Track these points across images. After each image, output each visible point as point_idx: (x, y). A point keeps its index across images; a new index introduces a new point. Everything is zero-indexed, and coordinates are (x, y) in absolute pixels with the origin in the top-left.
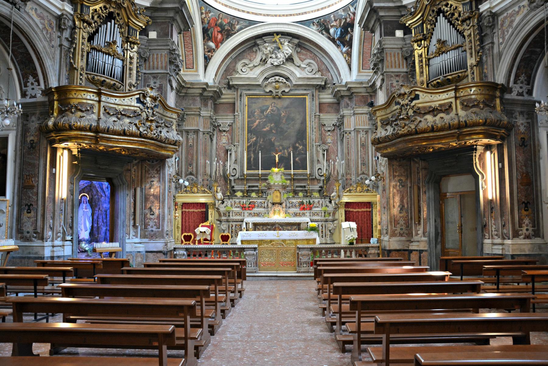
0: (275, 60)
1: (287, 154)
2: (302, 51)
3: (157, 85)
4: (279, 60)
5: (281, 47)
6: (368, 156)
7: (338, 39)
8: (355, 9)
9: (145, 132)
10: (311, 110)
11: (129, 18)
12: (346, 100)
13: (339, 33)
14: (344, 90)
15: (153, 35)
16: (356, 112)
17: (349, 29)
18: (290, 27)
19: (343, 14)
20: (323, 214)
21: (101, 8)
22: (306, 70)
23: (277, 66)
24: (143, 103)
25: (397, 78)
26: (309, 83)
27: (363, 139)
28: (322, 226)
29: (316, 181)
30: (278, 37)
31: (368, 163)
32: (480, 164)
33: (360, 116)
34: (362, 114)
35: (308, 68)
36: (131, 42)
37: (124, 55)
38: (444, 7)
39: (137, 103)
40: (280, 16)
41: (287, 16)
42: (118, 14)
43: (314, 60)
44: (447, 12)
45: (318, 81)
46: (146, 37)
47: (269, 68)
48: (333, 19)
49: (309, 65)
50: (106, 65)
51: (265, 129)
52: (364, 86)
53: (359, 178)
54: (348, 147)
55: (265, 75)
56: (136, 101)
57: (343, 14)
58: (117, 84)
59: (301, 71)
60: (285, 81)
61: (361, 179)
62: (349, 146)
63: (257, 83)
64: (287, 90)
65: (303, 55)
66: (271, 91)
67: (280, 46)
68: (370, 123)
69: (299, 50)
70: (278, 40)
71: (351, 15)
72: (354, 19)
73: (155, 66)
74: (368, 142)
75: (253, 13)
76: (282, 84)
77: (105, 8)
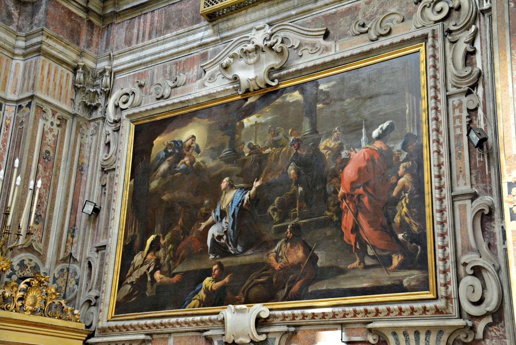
16: (44, 47)
31: (50, 218)
33: (54, 65)
34: (62, 62)
61: (22, 265)
68: (79, 99)
74: (60, 152)
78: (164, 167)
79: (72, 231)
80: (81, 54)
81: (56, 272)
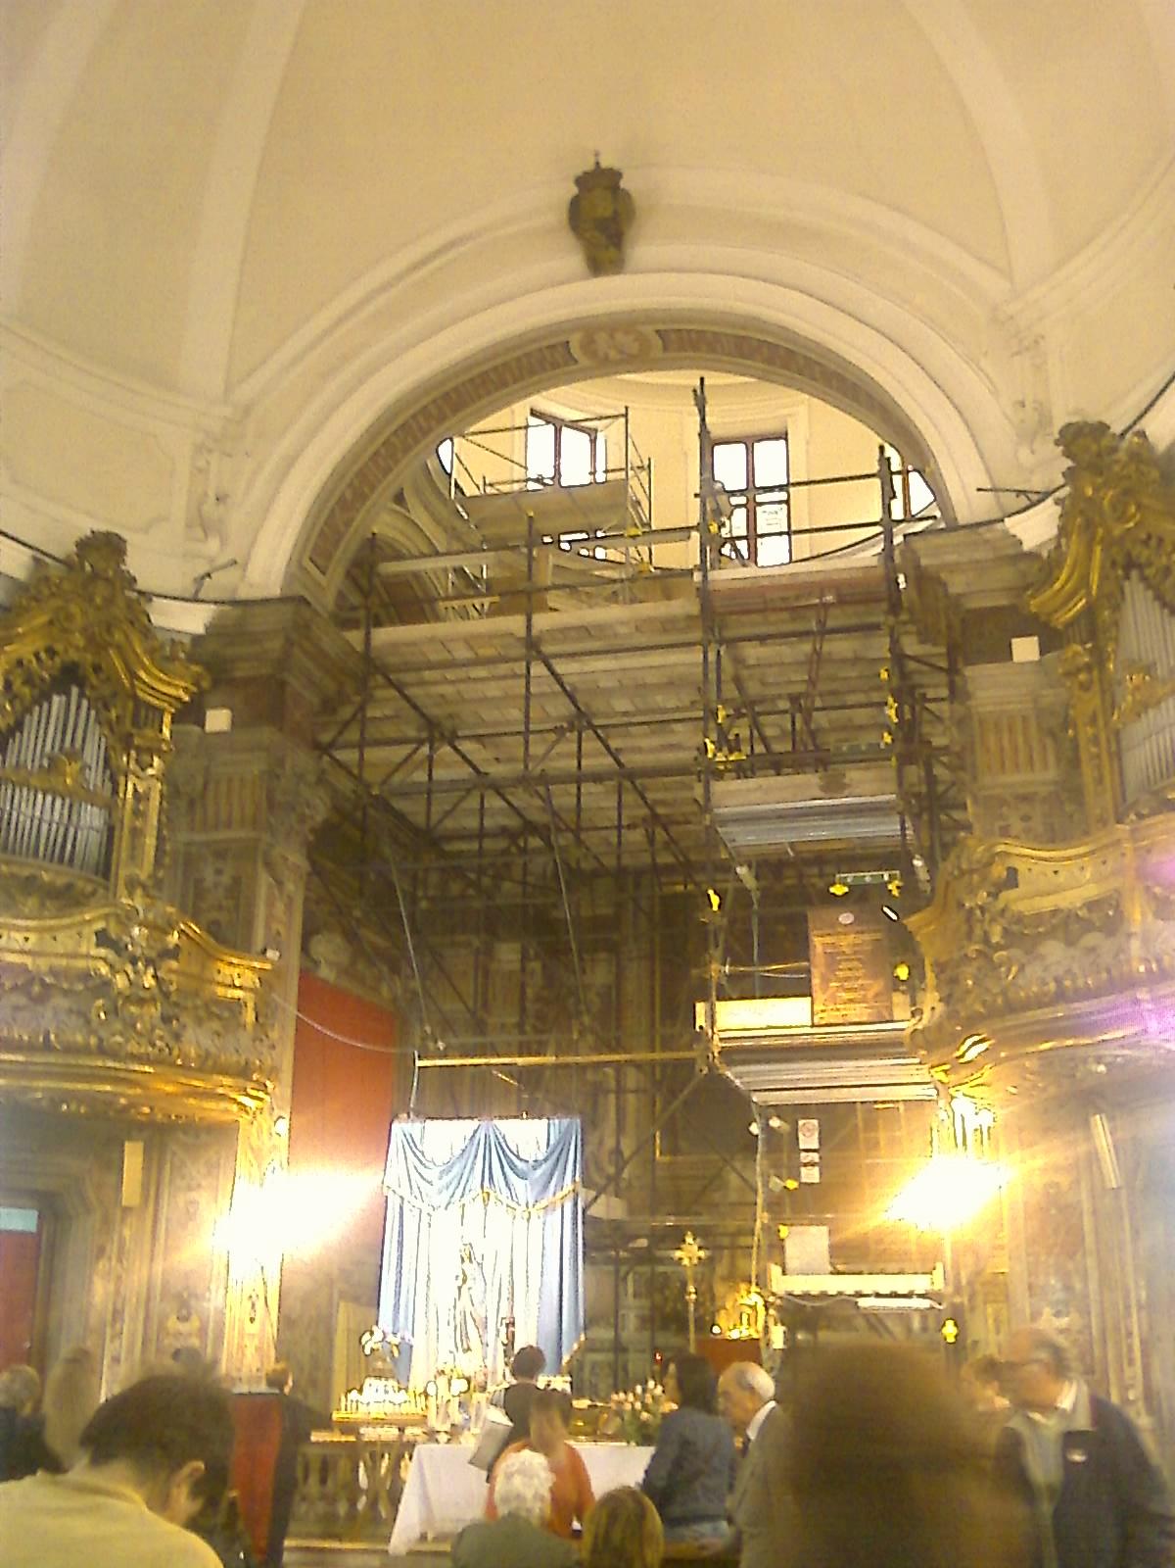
3: (226, 879)
9: (119, 1039)
11: (133, 676)
15: (218, 720)
21: (37, 655)
24: (117, 947)
25: (1025, 808)
36: (139, 750)
37: (115, 792)
39: (98, 945)
42: (97, 669)
44: (1150, 564)
46: (196, 729)
50: (45, 827)
56: (94, 938)
58: (80, 884)
73: (223, 816)
77: (51, 652)
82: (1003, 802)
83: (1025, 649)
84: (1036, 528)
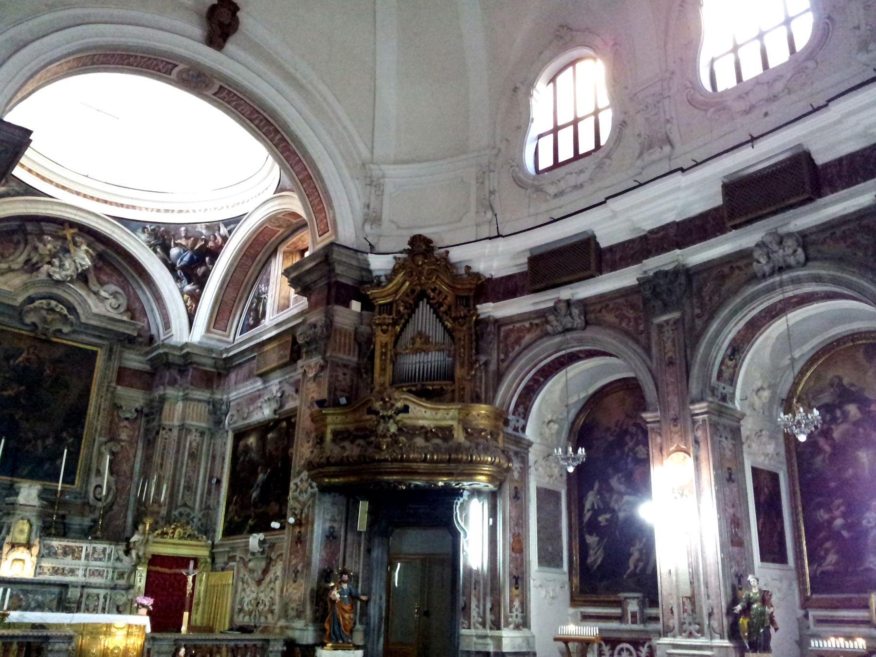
0: (57, 270)
1: (40, 449)
2: (105, 267)
4: (64, 273)
5: (72, 251)
6: (198, 476)
7: (182, 268)
8: (230, 232)
10: (104, 377)
12: (175, 372)
13: (186, 259)
14: (174, 355)
17: (207, 259)
18: (100, 221)
19: (204, 231)
20: (110, 575)
22: (108, 302)
23: (58, 282)
25: (345, 370)
26: (109, 327)
27: (194, 444)
28: (105, 598)
29: (87, 508)
30: (72, 231)
31: (197, 488)
32: (461, 516)
33: (196, 403)
34: (200, 401)
35: (112, 301)
38: (429, 291)
40: (85, 196)
41: (98, 200)
43: (123, 288)
45: (128, 329)
47: (42, 282)
48: (183, 234)
49: (114, 295)
51: (5, 393)
52: (214, 355)
53: (176, 513)
54: (163, 454)
55: (31, 292)
57: (204, 231)
59: (97, 302)
60: (65, 312)
61: (181, 514)
62: (165, 452)
63: (11, 302)
64: (66, 329)
65: (106, 274)
66: (34, 324)
67: (72, 247)
69: (100, 264)
70: (69, 237)
71: (219, 238)
72: (221, 247)
74: (202, 449)
75: (38, 175)
76: (58, 316)
78: (242, 458)
79: (209, 492)
80: (213, 393)
81: (200, 516)
82: (338, 365)
83: (356, 306)
84: (380, 264)
